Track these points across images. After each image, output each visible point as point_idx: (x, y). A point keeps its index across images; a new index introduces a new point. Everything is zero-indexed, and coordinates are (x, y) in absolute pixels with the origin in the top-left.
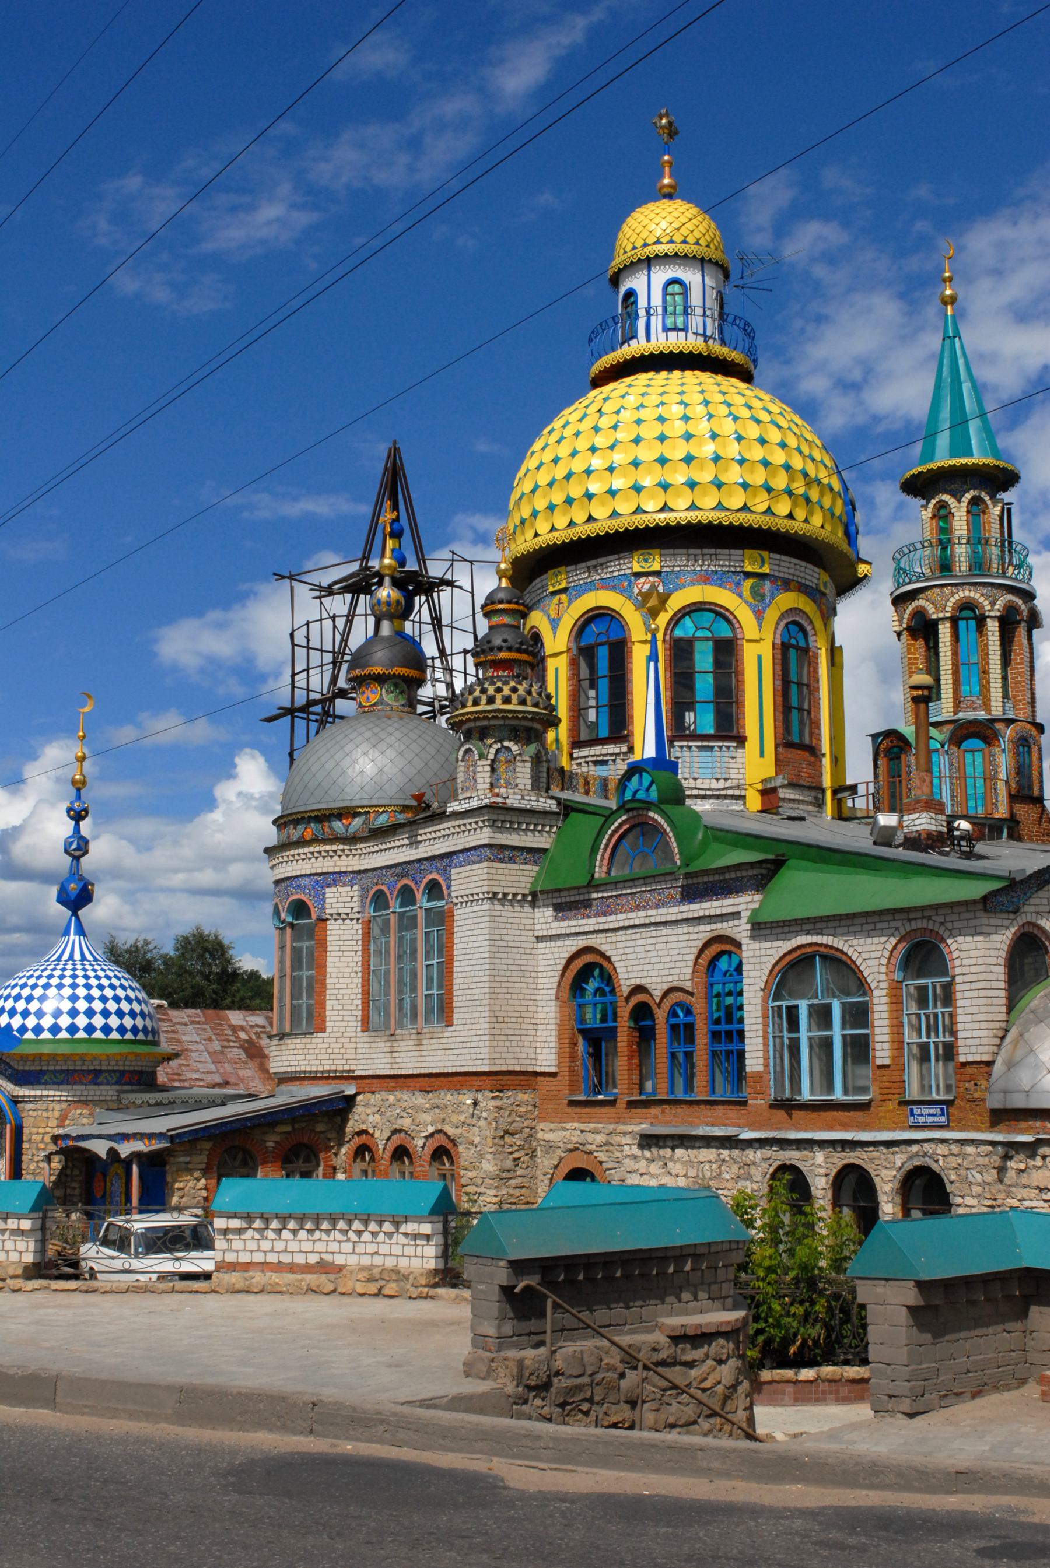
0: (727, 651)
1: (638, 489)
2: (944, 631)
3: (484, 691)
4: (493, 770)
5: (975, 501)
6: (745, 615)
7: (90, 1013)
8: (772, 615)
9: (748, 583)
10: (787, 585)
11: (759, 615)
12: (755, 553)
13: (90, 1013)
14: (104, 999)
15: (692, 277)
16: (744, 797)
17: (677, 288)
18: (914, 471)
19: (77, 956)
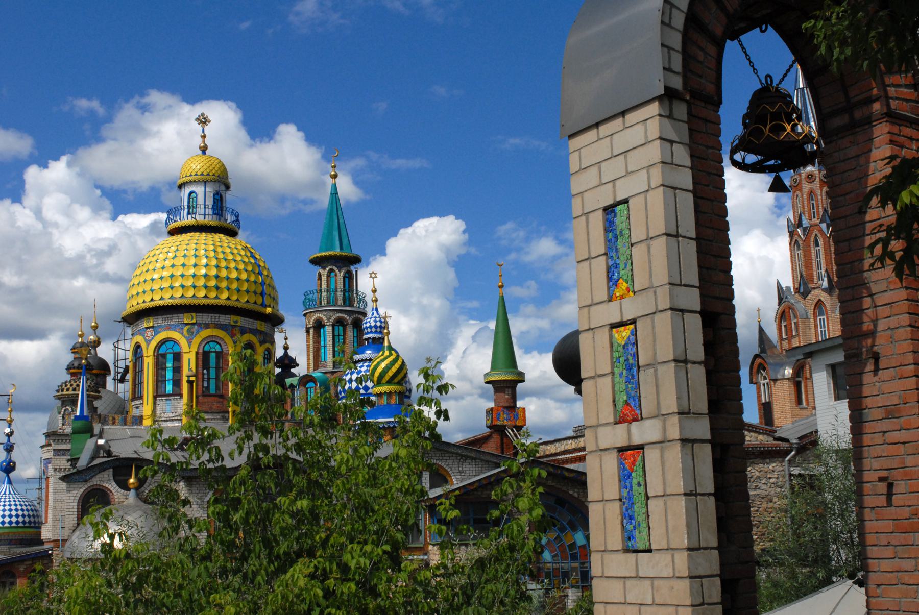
0: (177, 357)
1: (172, 288)
2: (311, 331)
3: (72, 385)
4: (63, 418)
5: (331, 271)
6: (183, 342)
7: (10, 516)
8: (197, 340)
9: (186, 328)
10: (207, 326)
11: (190, 342)
12: (189, 315)
13: (10, 516)
14: (22, 510)
15: (199, 189)
16: (181, 420)
17: (194, 195)
18: (315, 256)
19: (7, 493)
